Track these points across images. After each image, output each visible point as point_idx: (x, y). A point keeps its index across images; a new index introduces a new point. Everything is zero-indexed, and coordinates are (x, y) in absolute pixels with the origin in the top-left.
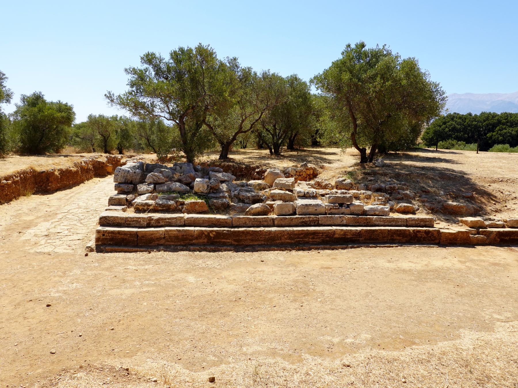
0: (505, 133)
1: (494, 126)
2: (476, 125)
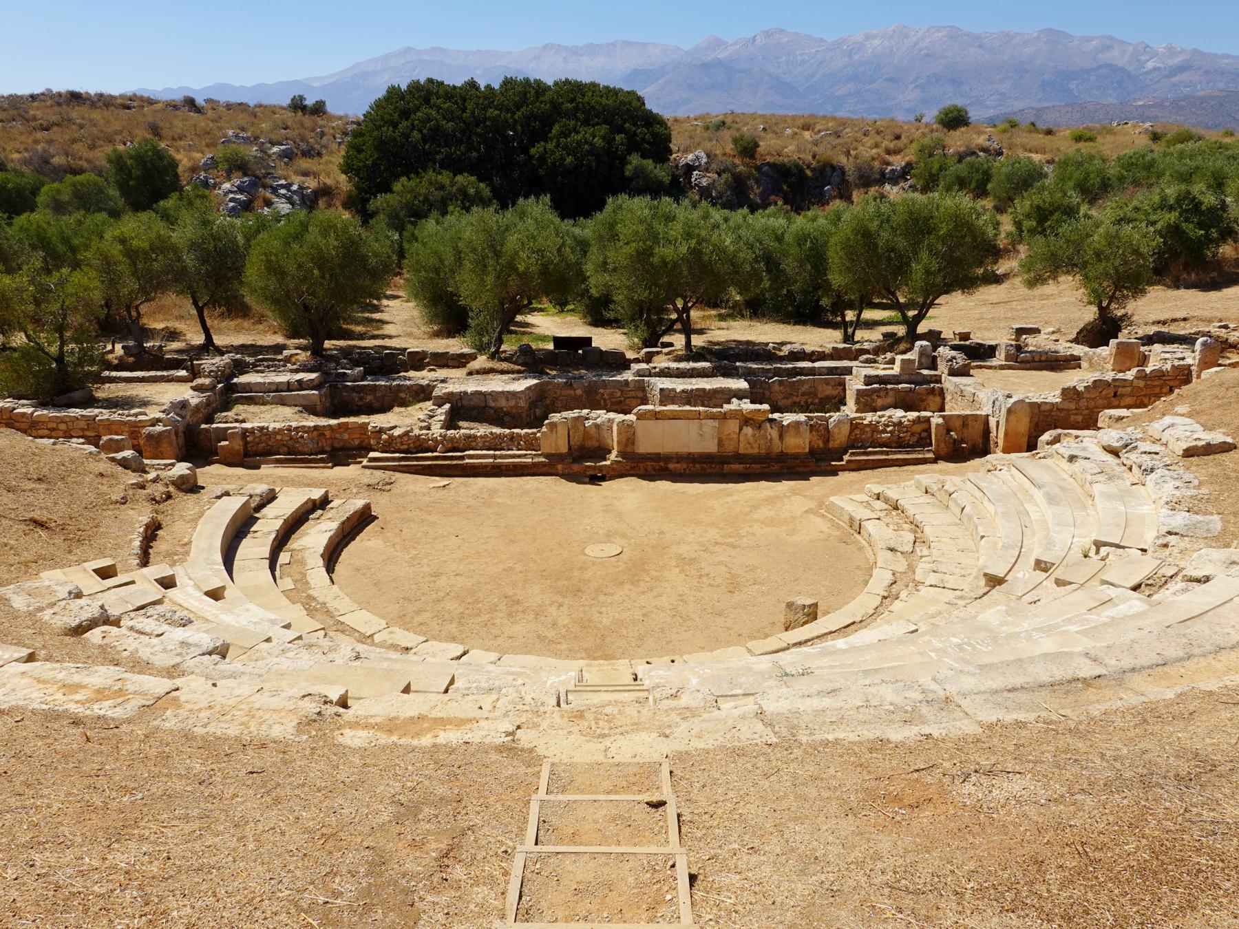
0: (579, 143)
2: (495, 120)
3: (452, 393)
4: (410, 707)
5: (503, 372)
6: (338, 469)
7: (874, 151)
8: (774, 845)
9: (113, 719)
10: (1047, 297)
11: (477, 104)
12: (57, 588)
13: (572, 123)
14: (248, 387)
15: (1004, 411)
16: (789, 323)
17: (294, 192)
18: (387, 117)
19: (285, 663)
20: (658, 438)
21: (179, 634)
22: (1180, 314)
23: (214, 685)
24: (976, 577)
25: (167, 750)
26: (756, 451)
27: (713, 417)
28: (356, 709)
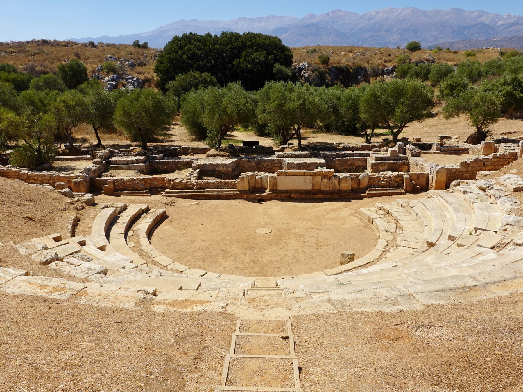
0: (254, 59)
1: (240, 50)
2: (218, 50)
3: (200, 165)
4: (182, 296)
5: (221, 156)
6: (153, 197)
7: (380, 61)
8: (335, 356)
9: (60, 300)
10: (454, 123)
11: (211, 43)
12: (37, 245)
13: (251, 50)
14: (115, 162)
15: (435, 172)
16: (343, 135)
17: (135, 81)
18: (173, 49)
19: (130, 277)
20: (286, 183)
21: (87, 265)
22: (513, 130)
23: (101, 286)
24: (423, 243)
25: (82, 312)
26: (328, 189)
27: (310, 175)
28: (160, 296)
